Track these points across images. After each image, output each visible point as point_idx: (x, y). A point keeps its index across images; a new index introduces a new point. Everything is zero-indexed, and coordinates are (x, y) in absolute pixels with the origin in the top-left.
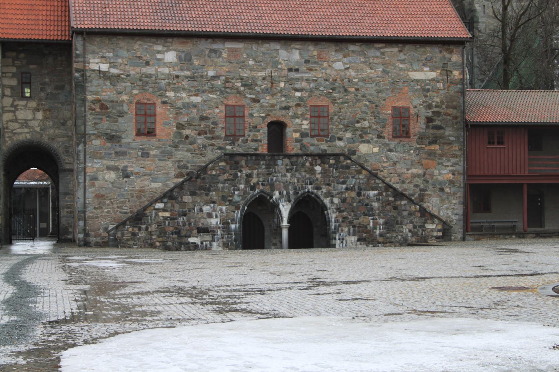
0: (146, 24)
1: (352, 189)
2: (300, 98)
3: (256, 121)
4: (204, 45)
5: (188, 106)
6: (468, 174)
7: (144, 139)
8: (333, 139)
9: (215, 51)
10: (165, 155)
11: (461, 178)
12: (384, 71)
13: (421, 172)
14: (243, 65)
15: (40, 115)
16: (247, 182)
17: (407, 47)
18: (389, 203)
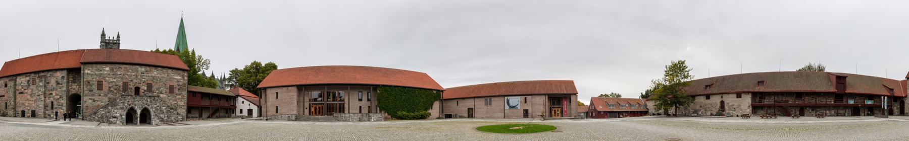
0: (101, 60)
4: (117, 66)
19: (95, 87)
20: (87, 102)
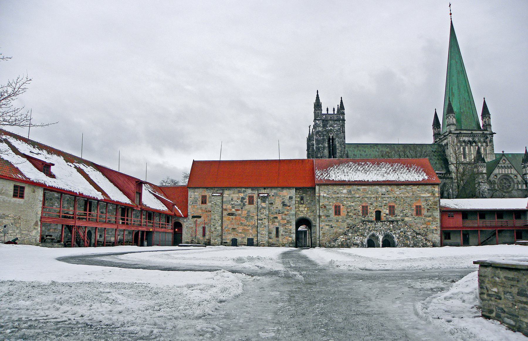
1: (402, 232)
2: (386, 203)
3: (371, 211)
4: (355, 187)
5: (350, 206)
6: (442, 227)
7: (337, 216)
8: (396, 216)
9: (358, 189)
10: (344, 221)
11: (439, 228)
12: (413, 194)
13: (425, 226)
14: (367, 193)
15: (306, 209)
16: (369, 230)
17: (420, 186)
18: (414, 236)
19: (332, 212)
20: (322, 229)
